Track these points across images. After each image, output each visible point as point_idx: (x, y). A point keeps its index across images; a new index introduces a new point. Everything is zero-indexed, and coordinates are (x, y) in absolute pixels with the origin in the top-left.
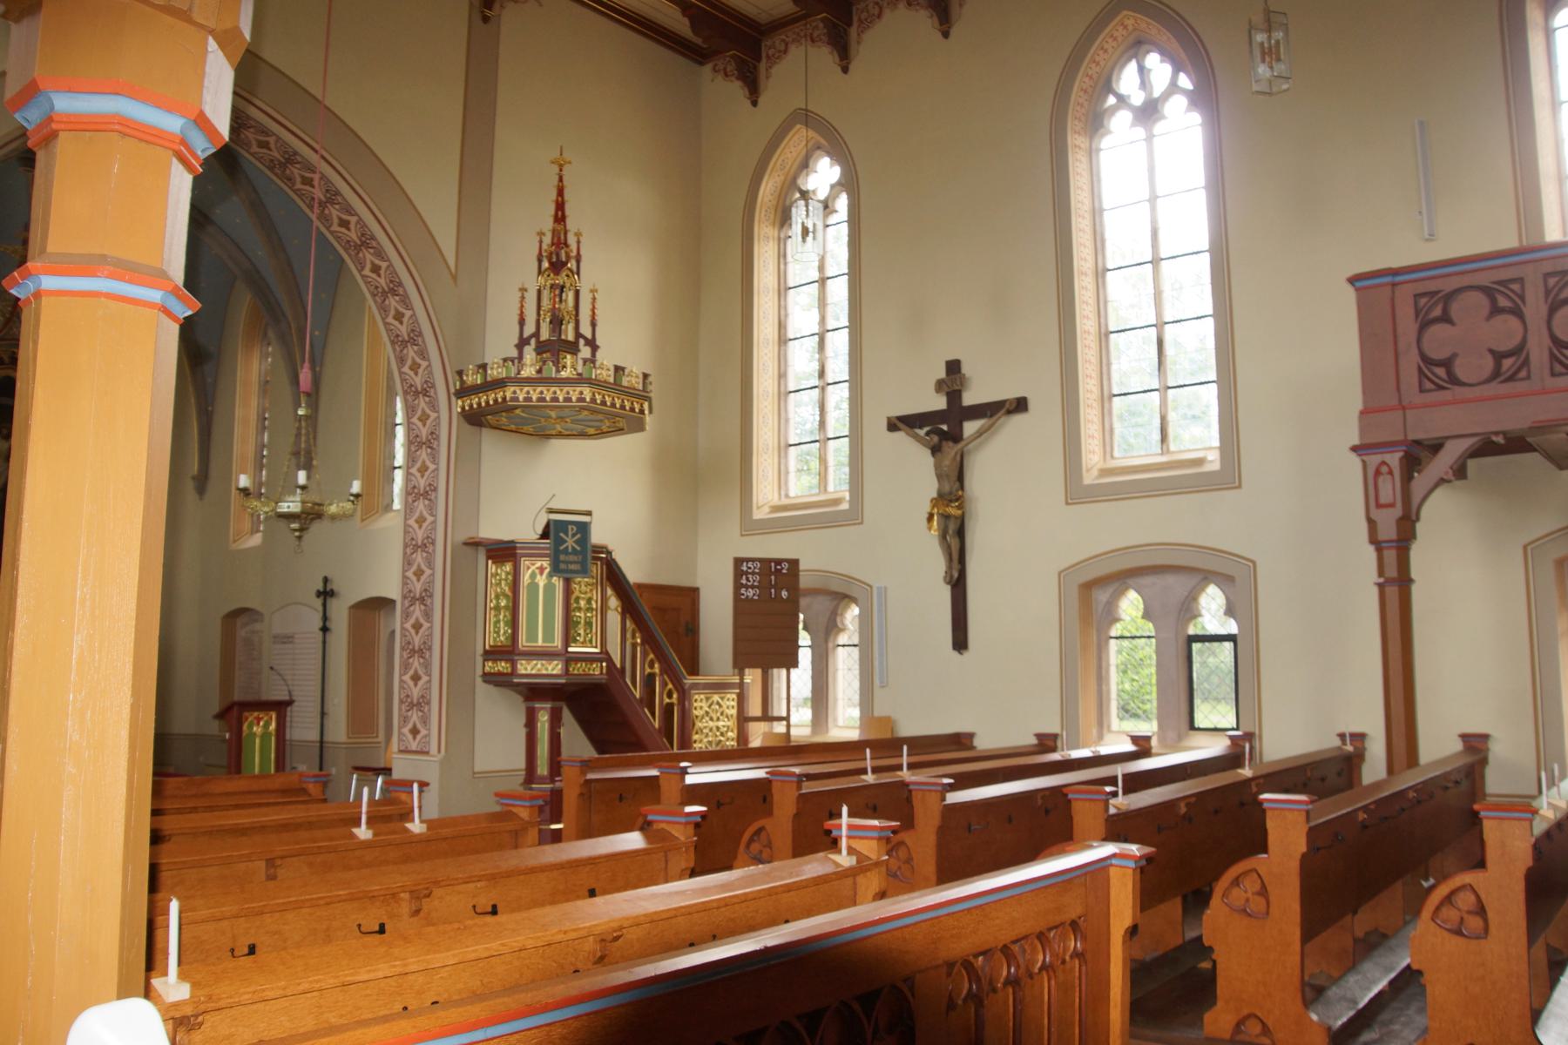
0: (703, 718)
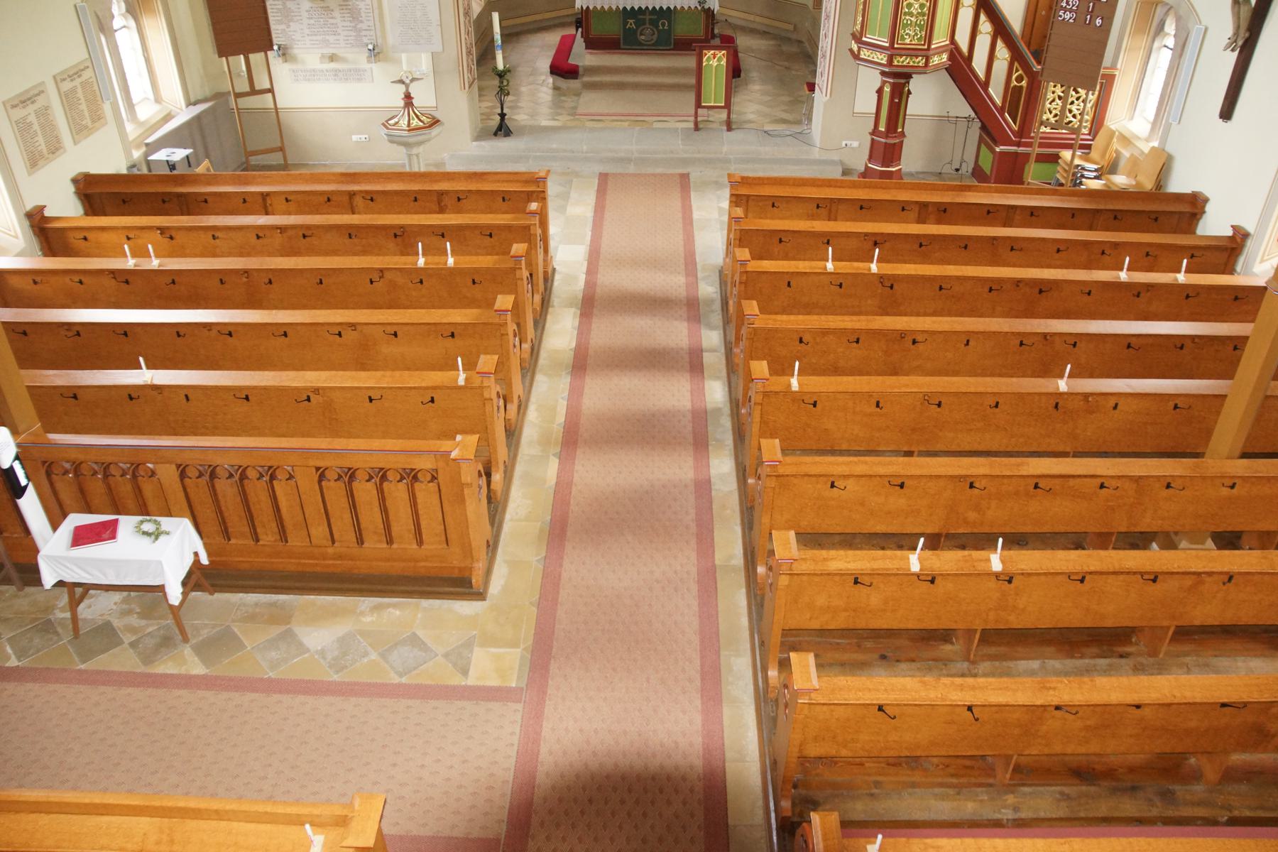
0: (1053, 101)
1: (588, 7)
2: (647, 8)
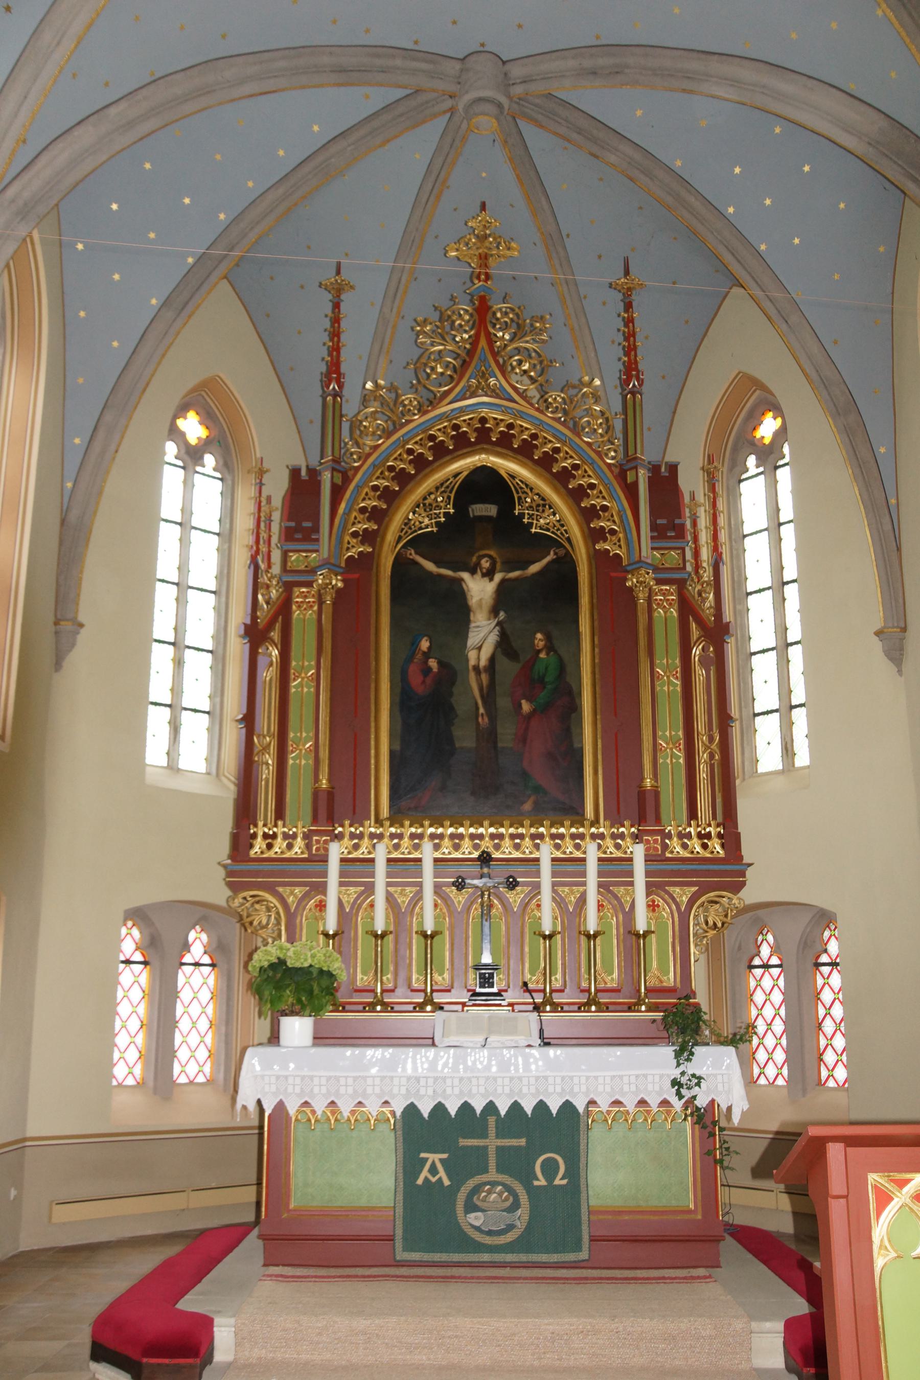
1: (280, 1107)
2: (491, 1107)
